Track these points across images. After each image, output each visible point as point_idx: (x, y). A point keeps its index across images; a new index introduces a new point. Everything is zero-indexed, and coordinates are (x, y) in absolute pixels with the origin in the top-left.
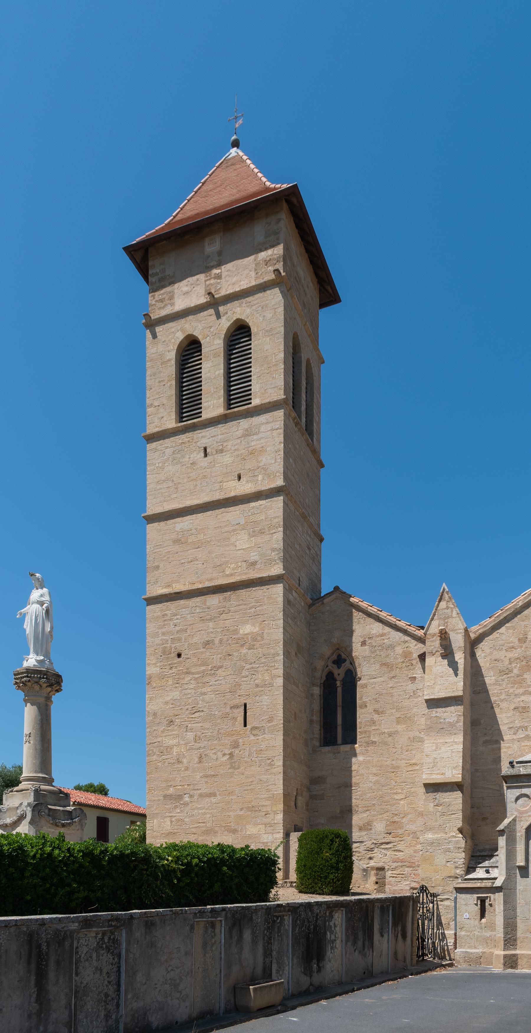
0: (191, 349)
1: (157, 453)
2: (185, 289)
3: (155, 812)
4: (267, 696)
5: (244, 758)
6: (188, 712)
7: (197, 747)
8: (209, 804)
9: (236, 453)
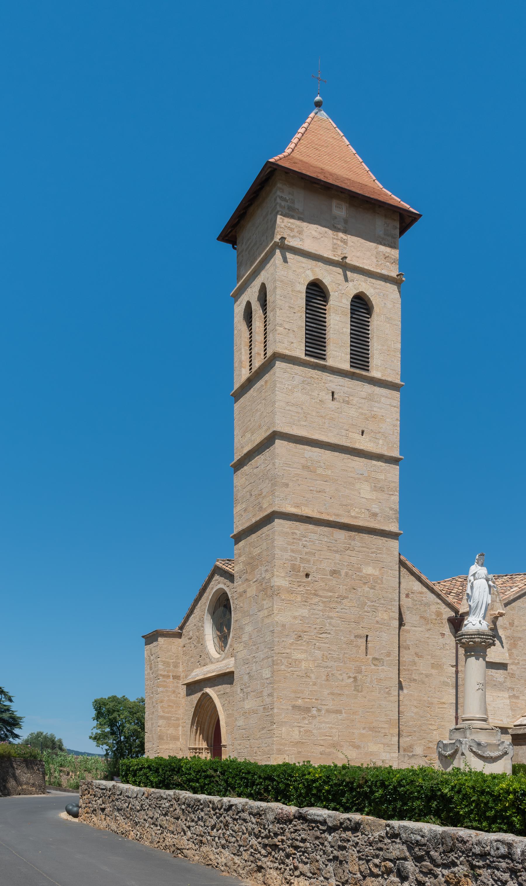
0: (317, 292)
1: (286, 375)
2: (315, 234)
3: (284, 720)
4: (385, 633)
5: (366, 683)
6: (315, 631)
7: (324, 666)
8: (336, 720)
9: (360, 410)
